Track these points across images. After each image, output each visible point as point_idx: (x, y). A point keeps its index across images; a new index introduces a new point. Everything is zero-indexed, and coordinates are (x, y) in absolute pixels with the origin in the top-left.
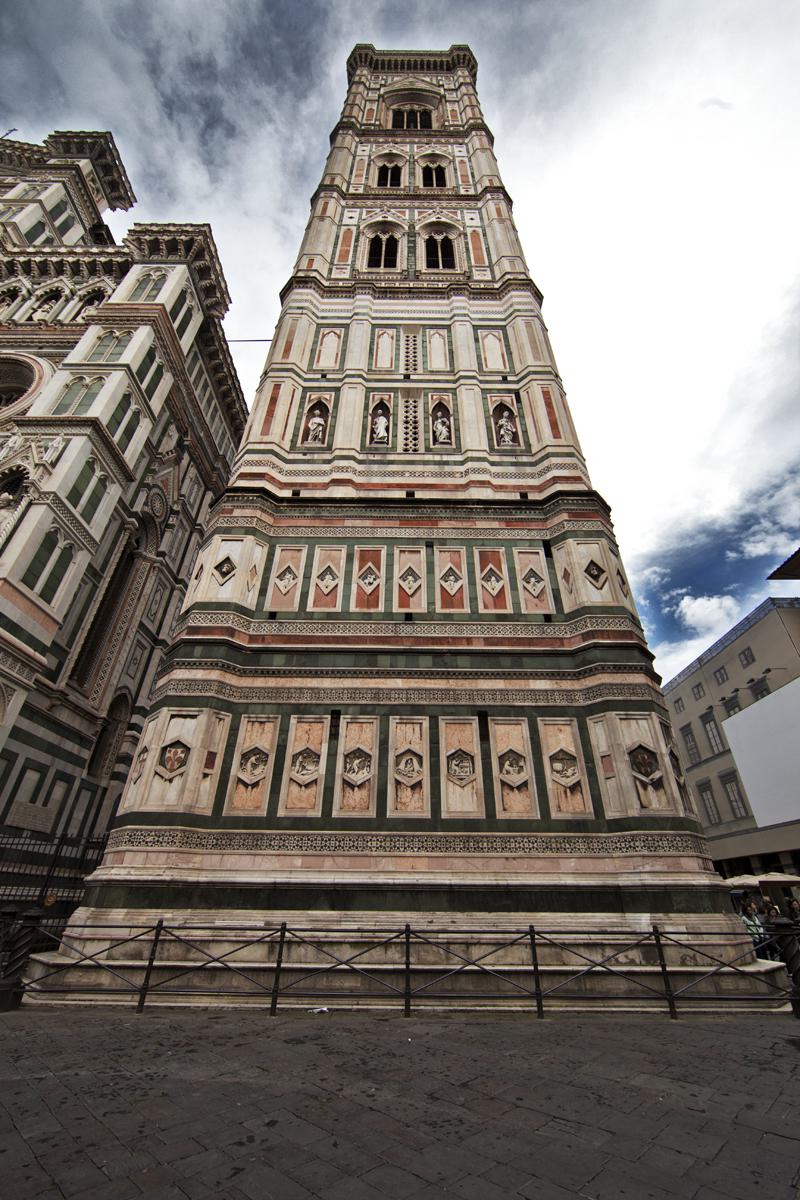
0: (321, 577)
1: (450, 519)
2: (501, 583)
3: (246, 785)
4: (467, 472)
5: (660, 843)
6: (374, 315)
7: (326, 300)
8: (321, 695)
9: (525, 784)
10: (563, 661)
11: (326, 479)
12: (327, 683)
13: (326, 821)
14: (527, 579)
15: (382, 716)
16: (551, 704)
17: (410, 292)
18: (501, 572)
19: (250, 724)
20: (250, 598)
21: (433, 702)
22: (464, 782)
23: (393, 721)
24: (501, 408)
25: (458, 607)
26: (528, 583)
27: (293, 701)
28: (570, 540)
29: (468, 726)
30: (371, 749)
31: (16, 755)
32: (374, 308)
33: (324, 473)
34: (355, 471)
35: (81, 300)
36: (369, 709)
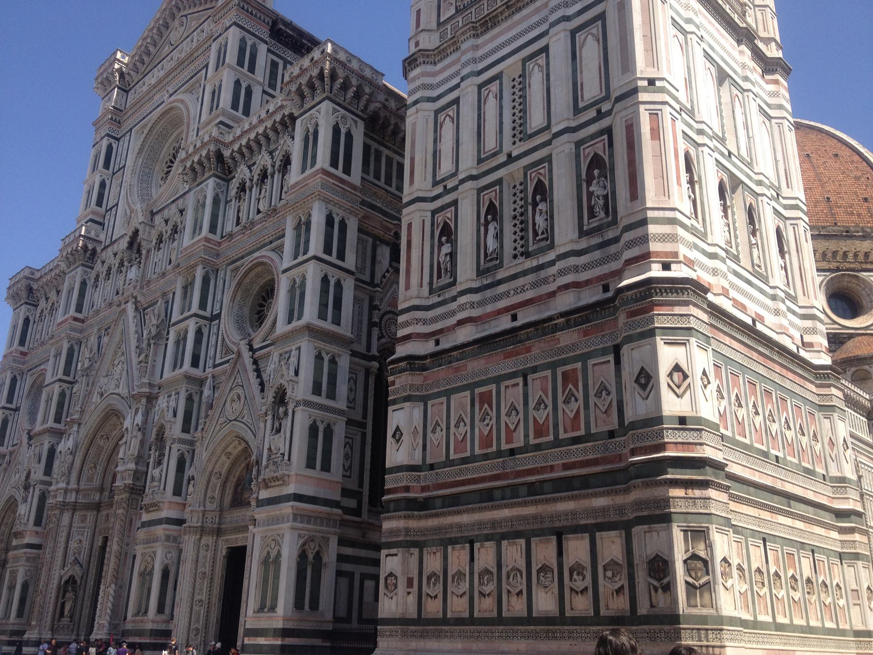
3: (431, 597)
5: (659, 635)
6: (481, 66)
7: (440, 66)
9: (586, 589)
12: (465, 519)
13: (471, 621)
14: (598, 395)
15: (497, 541)
17: (507, 7)
18: (578, 391)
20: (416, 456)
22: (547, 590)
24: (596, 162)
27: (448, 536)
31: (353, 573)
32: (480, 53)
33: (453, 313)
34: (472, 305)
35: (279, 171)
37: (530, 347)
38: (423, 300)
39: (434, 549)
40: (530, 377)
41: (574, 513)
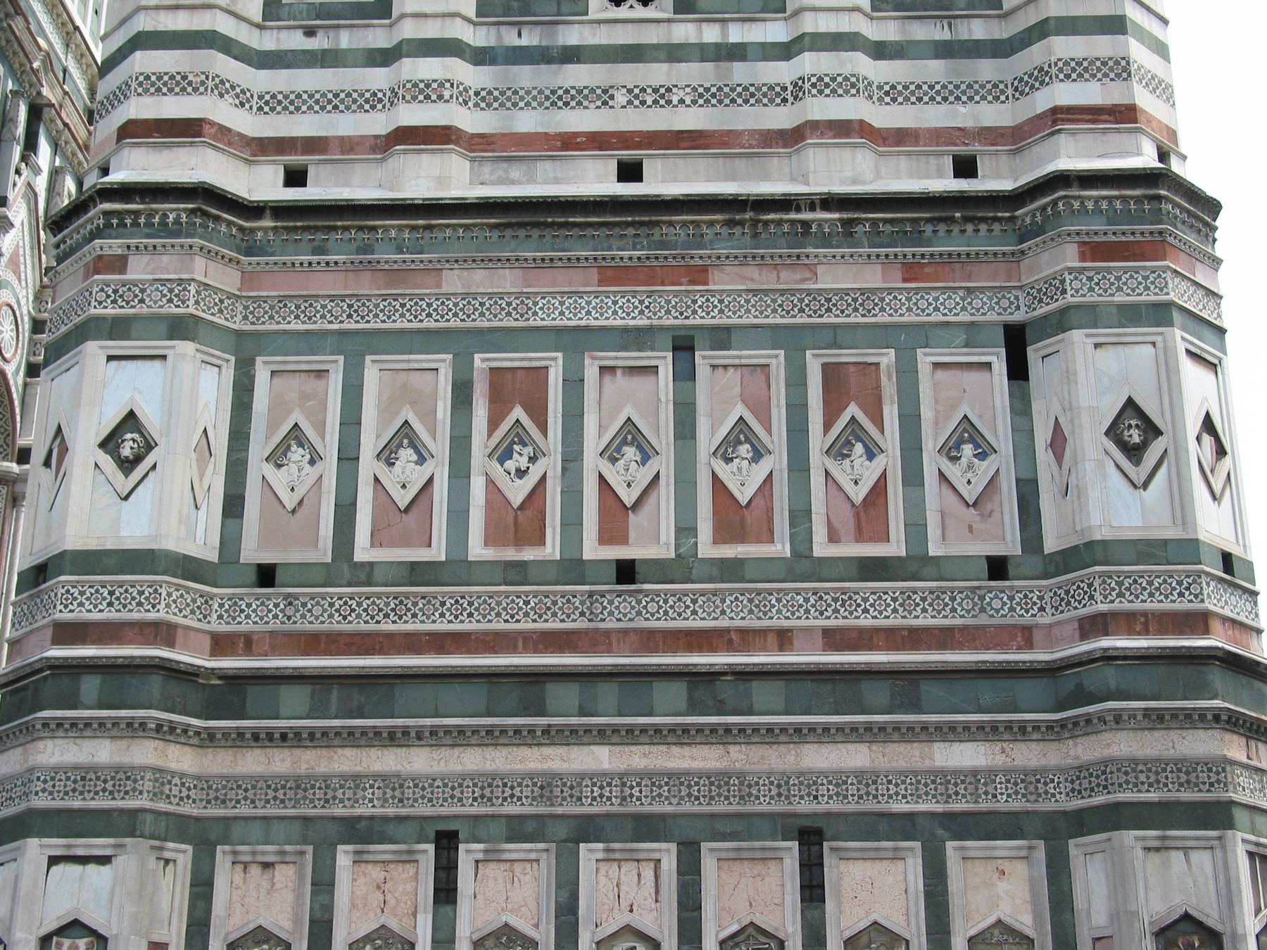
0: (388, 455)
1: (743, 261)
2: (880, 462)
4: (798, 90)
8: (409, 793)
10: (1025, 689)
11: (378, 124)
12: (419, 761)
14: (951, 451)
16: (983, 806)
18: (882, 431)
19: (239, 868)
21: (689, 807)
23: (589, 853)
25: (759, 541)
26: (954, 459)
27: (339, 811)
28: (1077, 335)
29: (773, 866)
30: (536, 926)
33: (372, 101)
34: (464, 97)
36: (530, 827)
37: (704, 270)
38: (244, 26)
39: (269, 851)
40: (702, 359)
41: (866, 778)
